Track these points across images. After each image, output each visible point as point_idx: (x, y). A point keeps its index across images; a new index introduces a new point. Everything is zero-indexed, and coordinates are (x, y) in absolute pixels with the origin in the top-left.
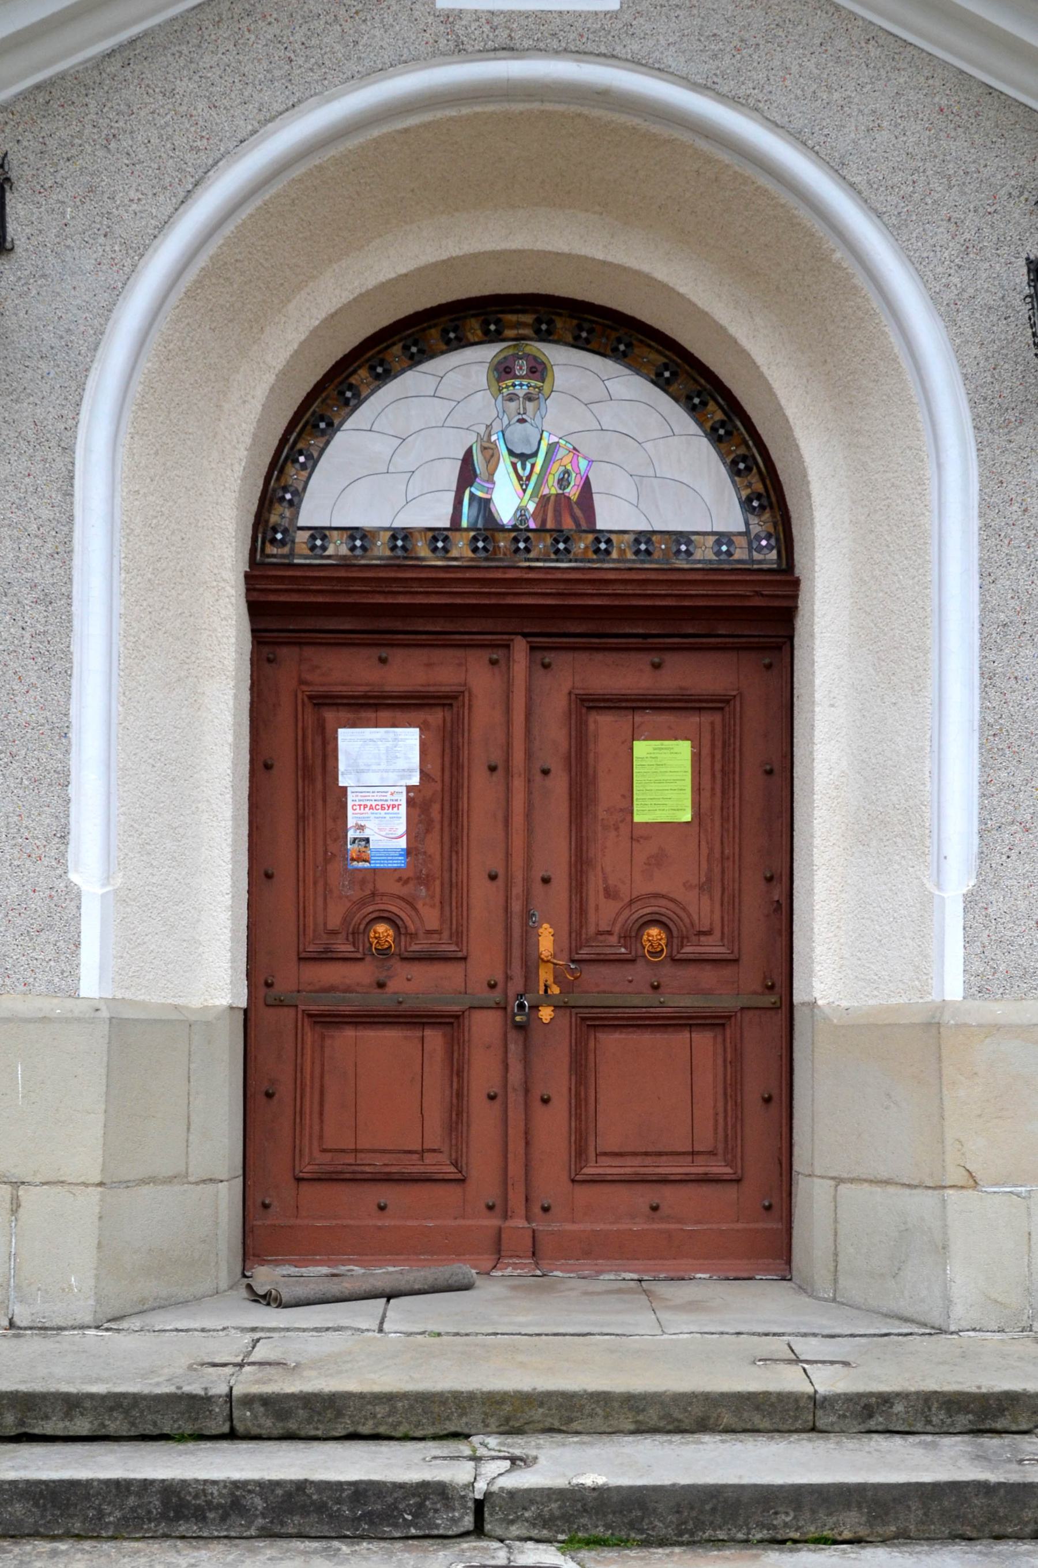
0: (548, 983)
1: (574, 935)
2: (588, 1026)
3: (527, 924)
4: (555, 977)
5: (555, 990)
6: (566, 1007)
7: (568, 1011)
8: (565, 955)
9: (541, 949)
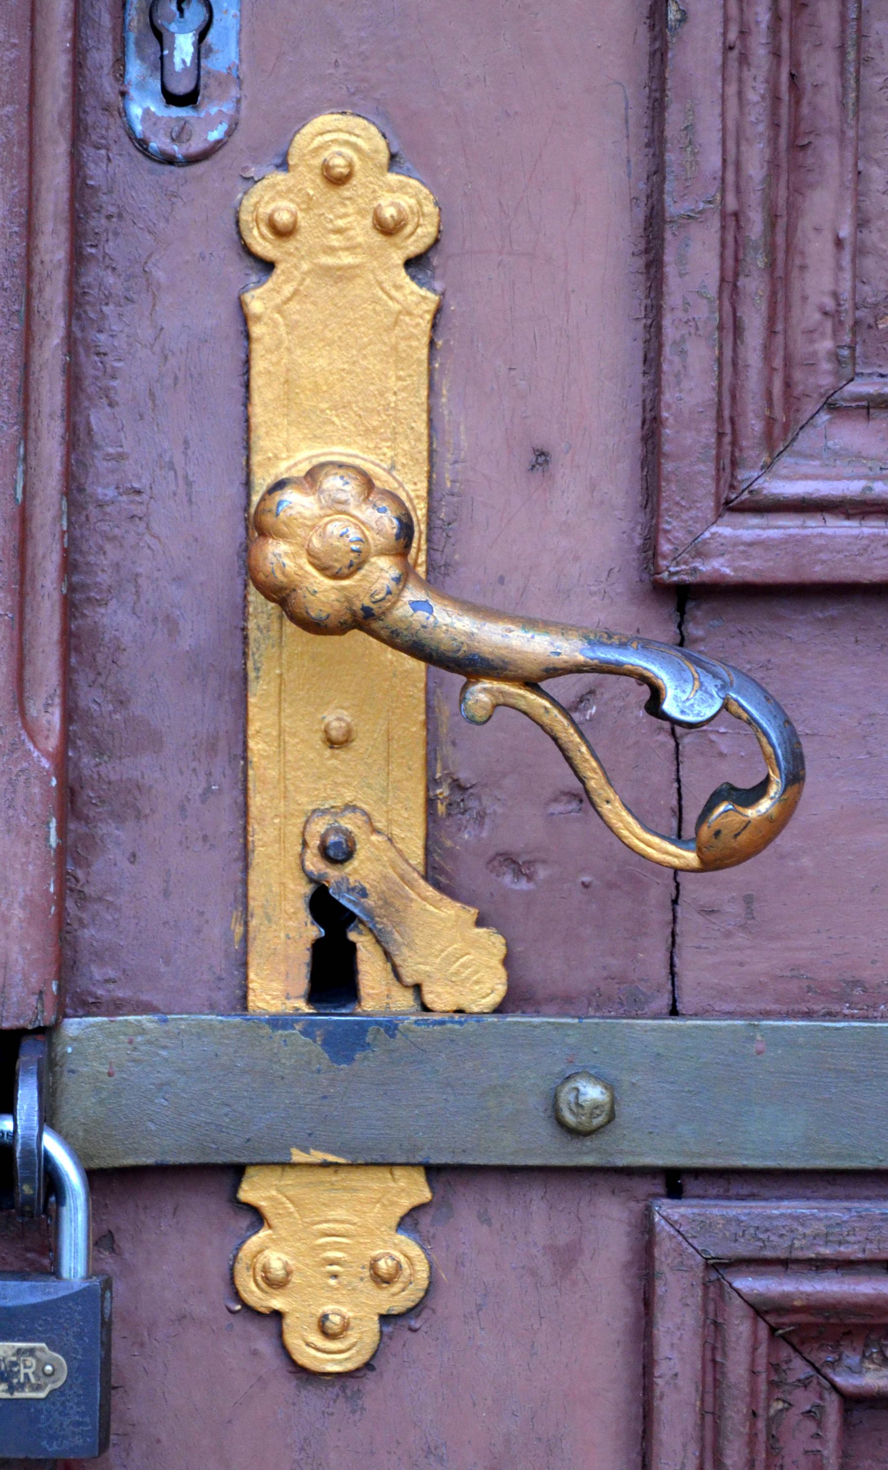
0: (365, 869)
1: (696, 261)
2: (852, 1402)
3: (88, 115)
4: (448, 800)
5: (449, 959)
6: (576, 1169)
7: (608, 1223)
8: (583, 522)
9: (282, 449)
